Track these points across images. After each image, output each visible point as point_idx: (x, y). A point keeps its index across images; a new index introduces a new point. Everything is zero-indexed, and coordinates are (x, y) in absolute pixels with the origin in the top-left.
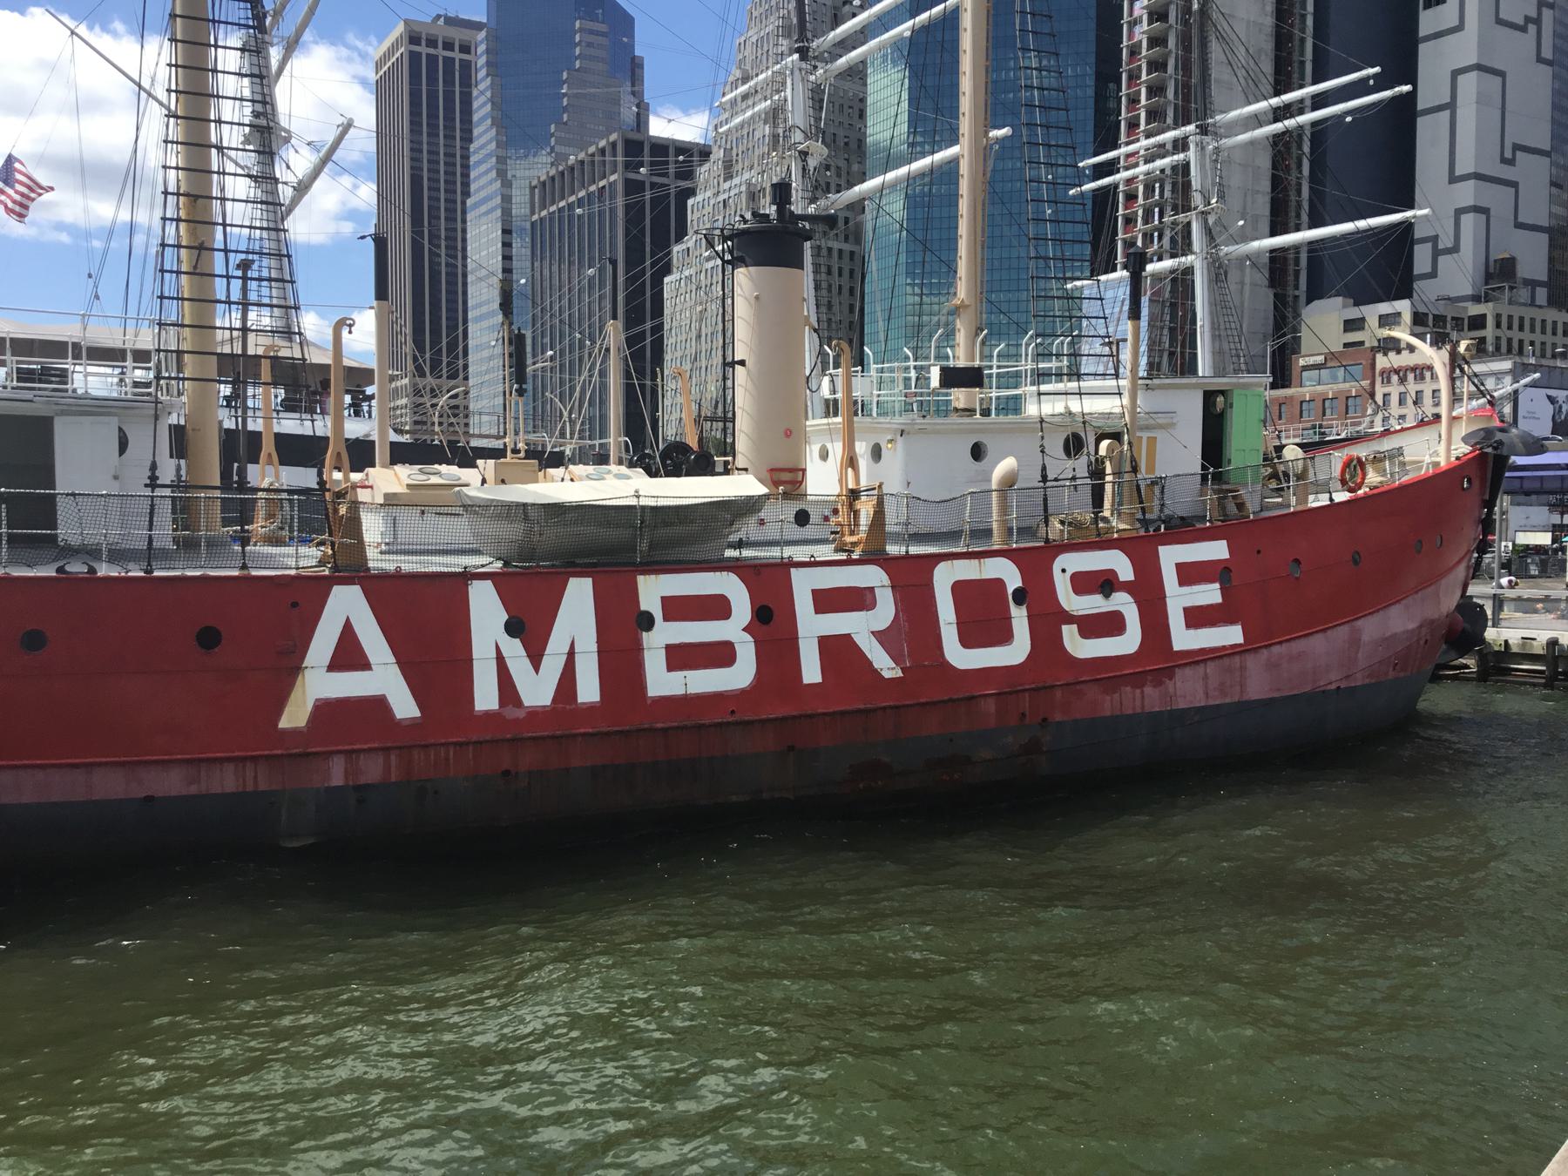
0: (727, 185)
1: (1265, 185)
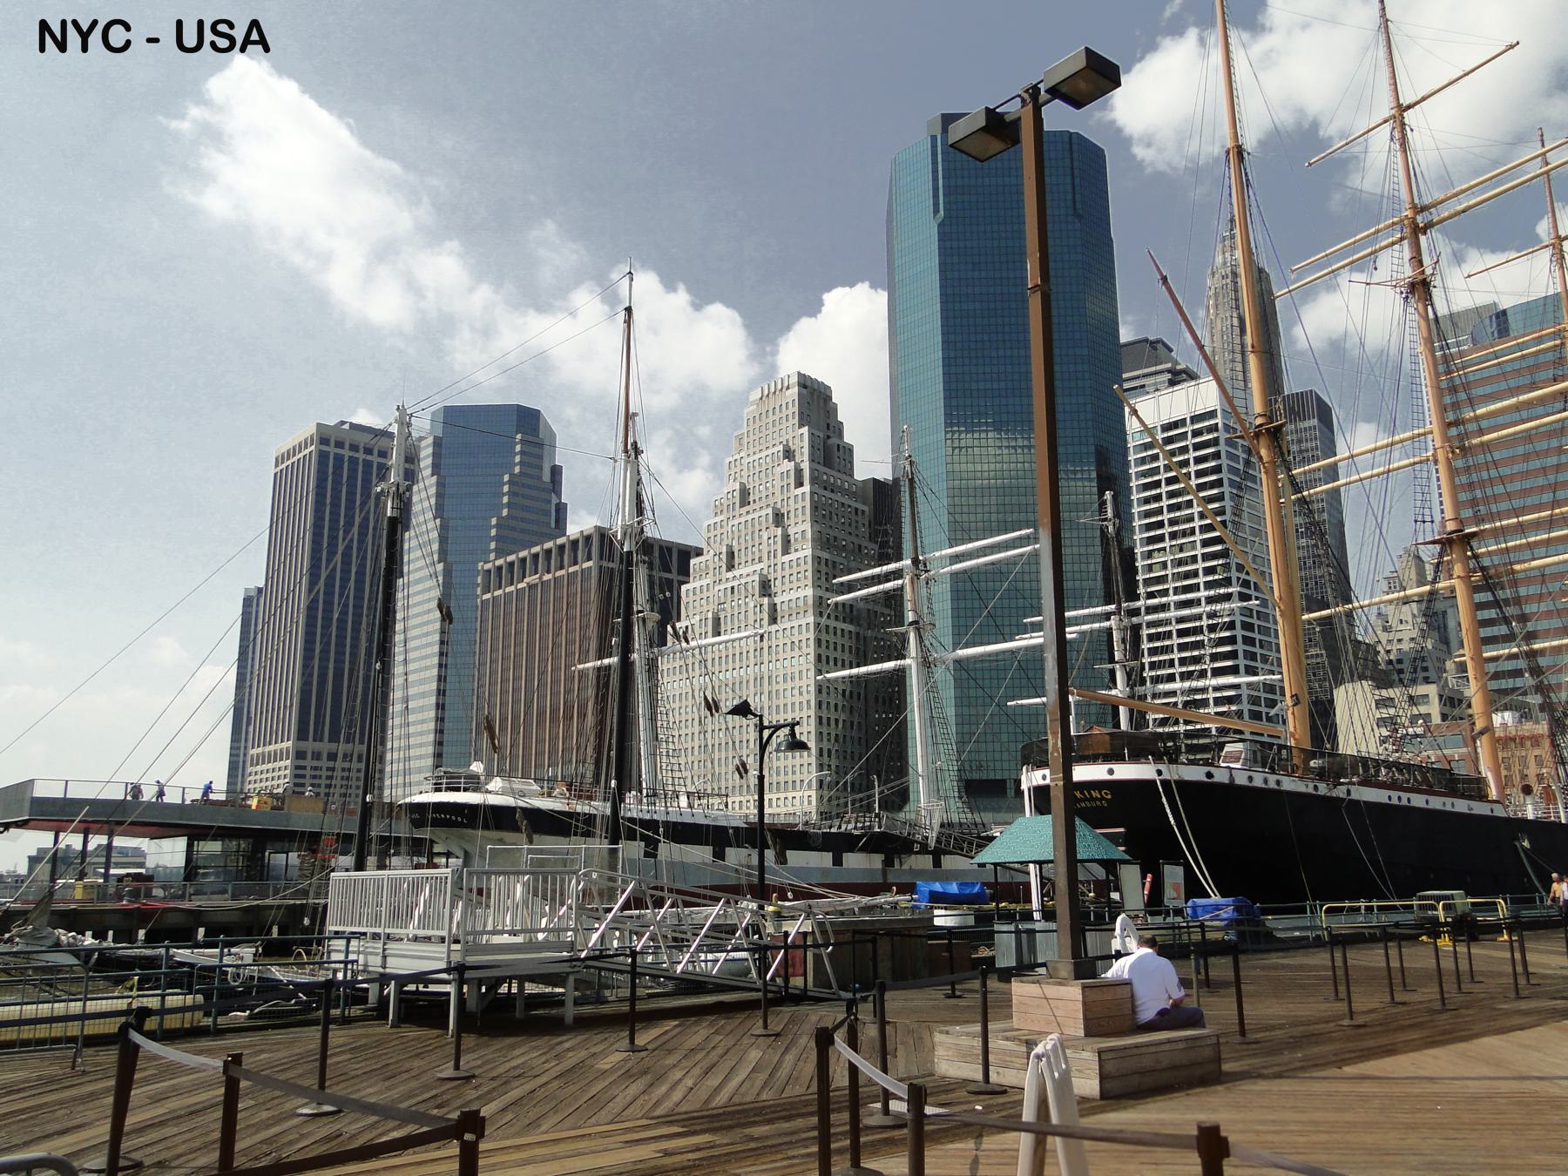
0: (730, 575)
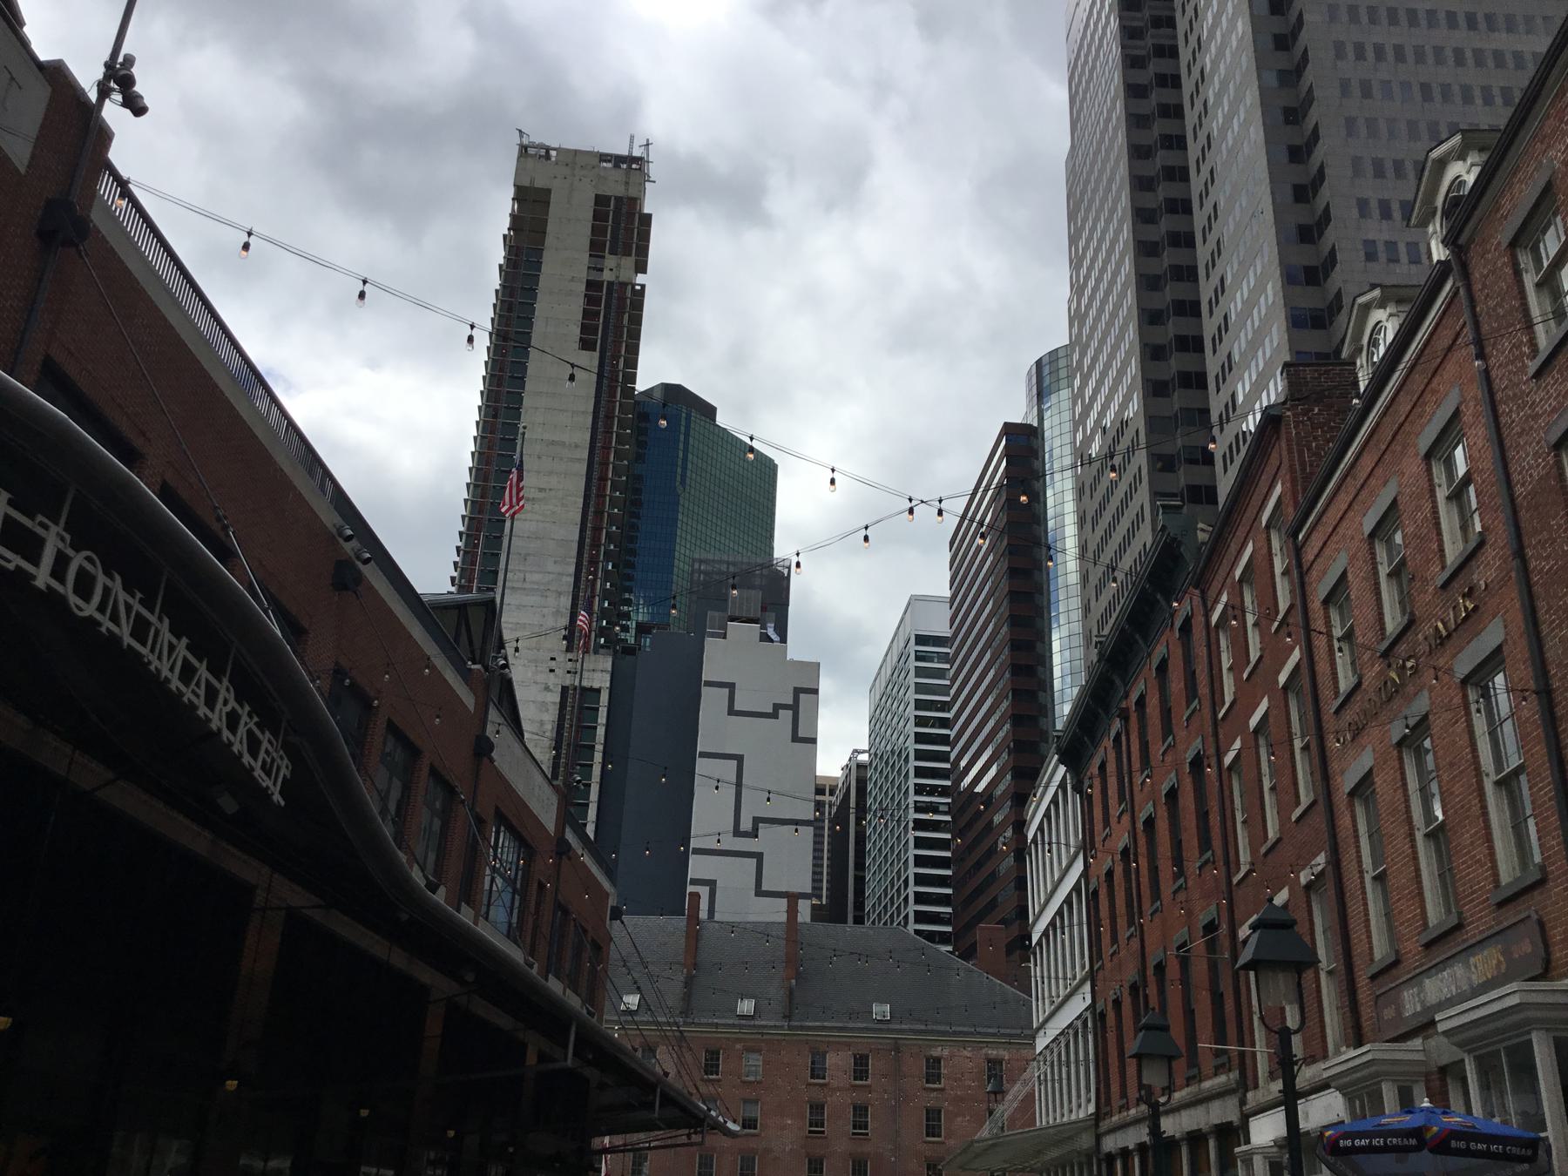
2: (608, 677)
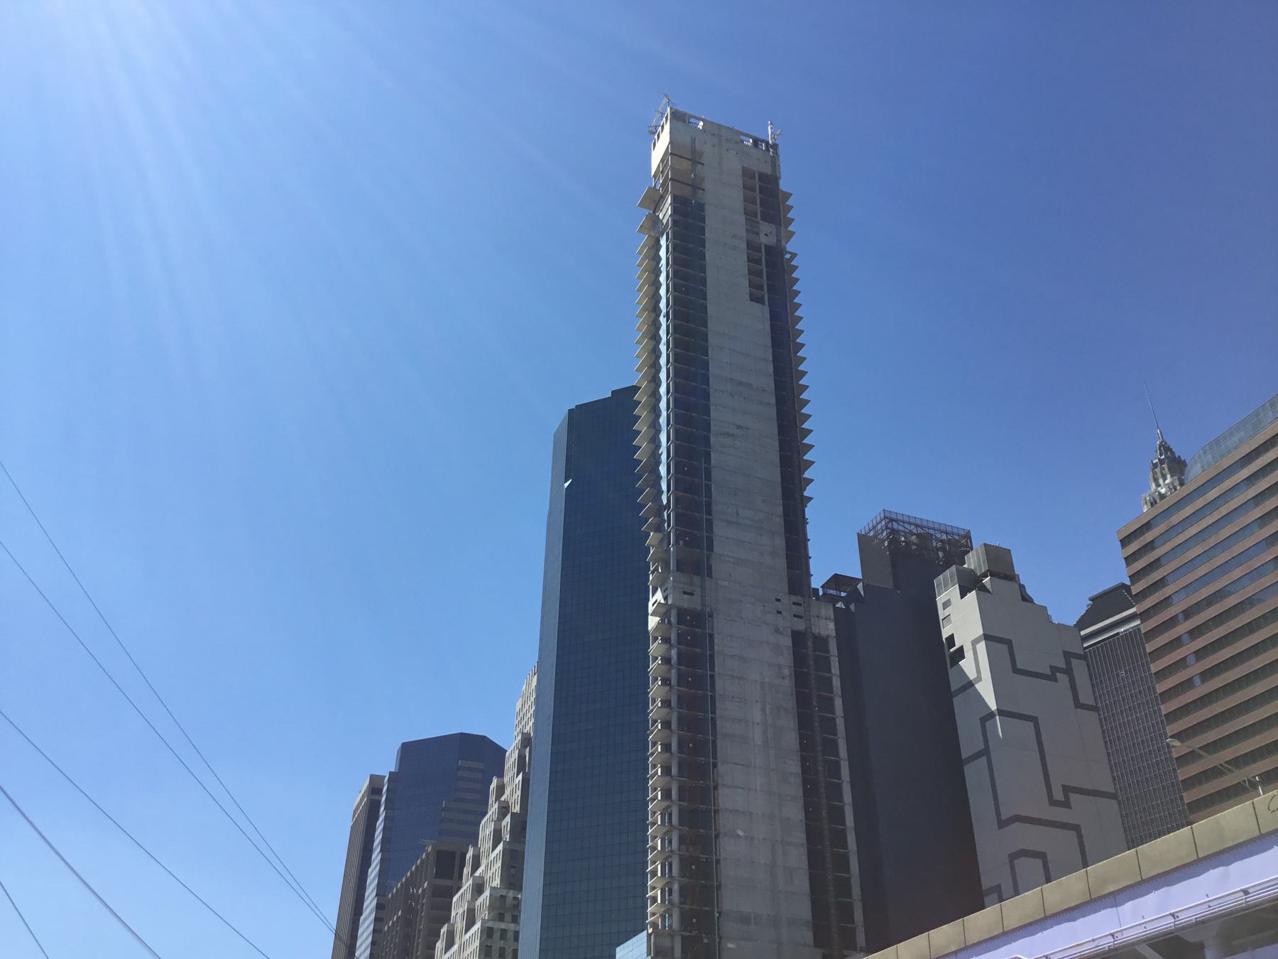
1: (800, 836)
2: (832, 626)
